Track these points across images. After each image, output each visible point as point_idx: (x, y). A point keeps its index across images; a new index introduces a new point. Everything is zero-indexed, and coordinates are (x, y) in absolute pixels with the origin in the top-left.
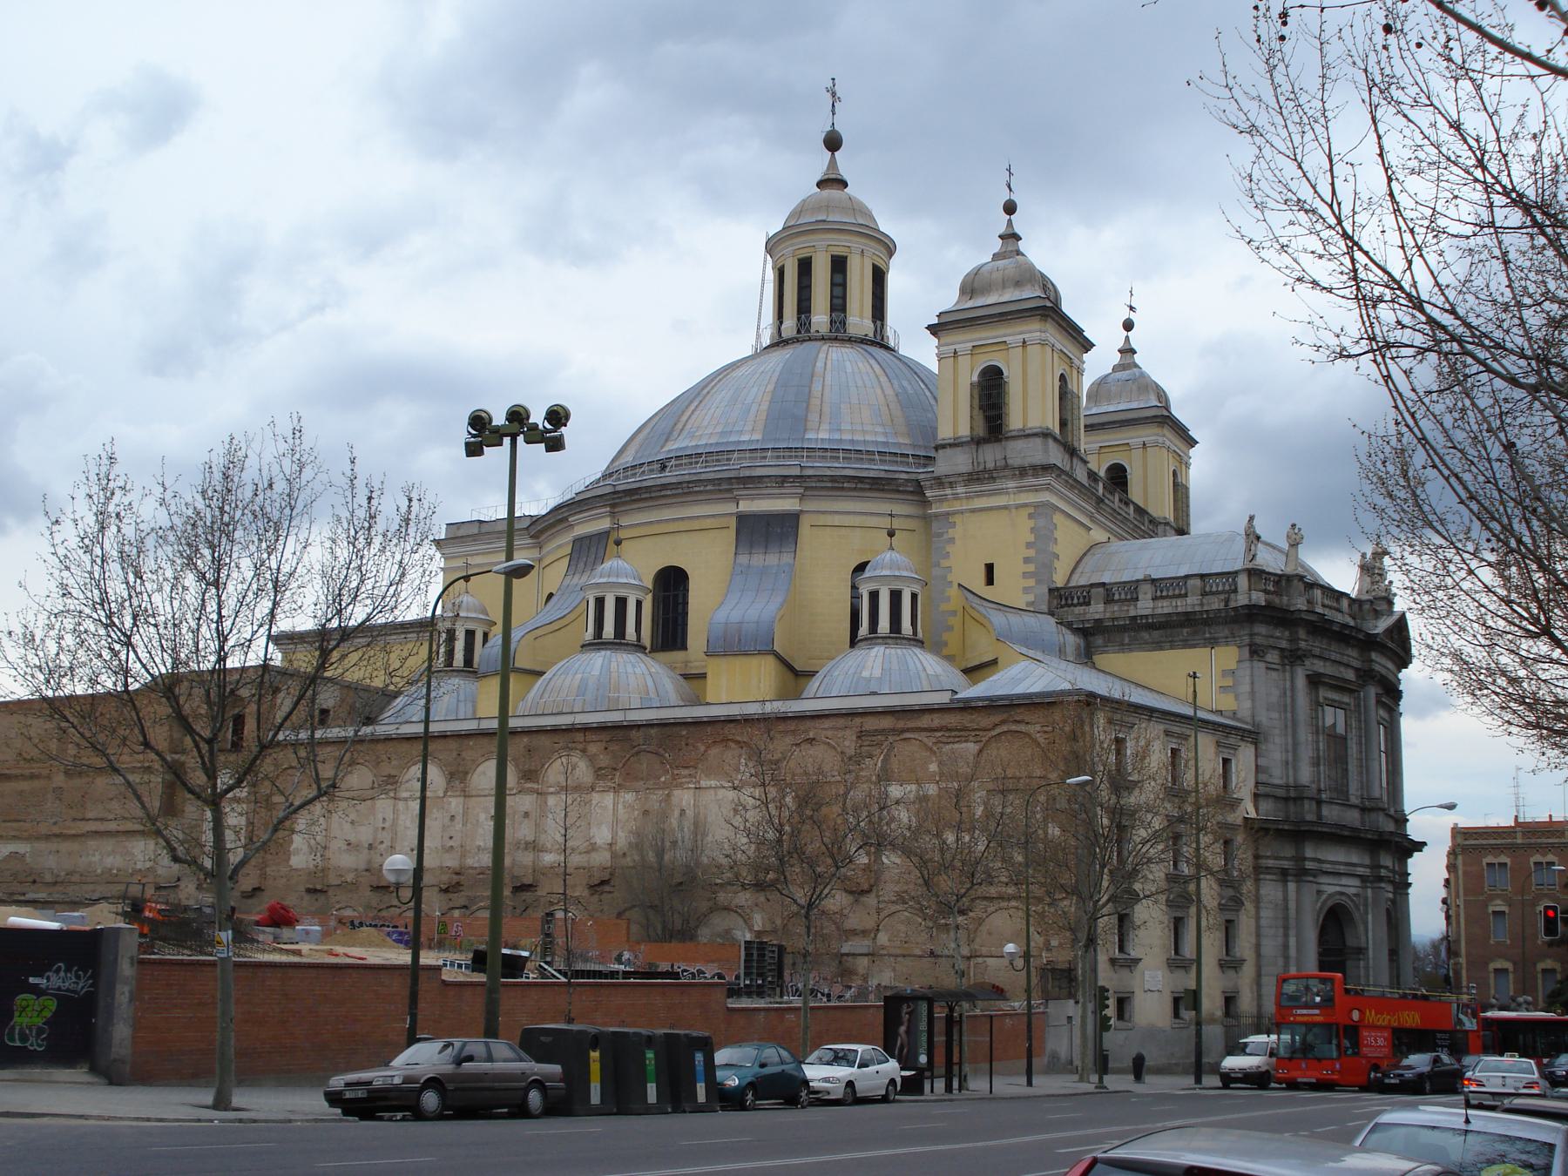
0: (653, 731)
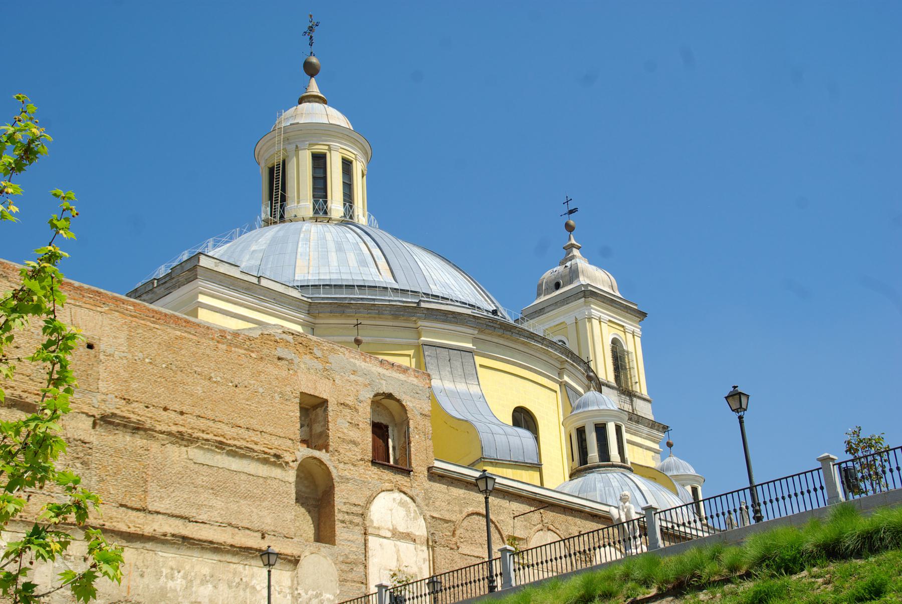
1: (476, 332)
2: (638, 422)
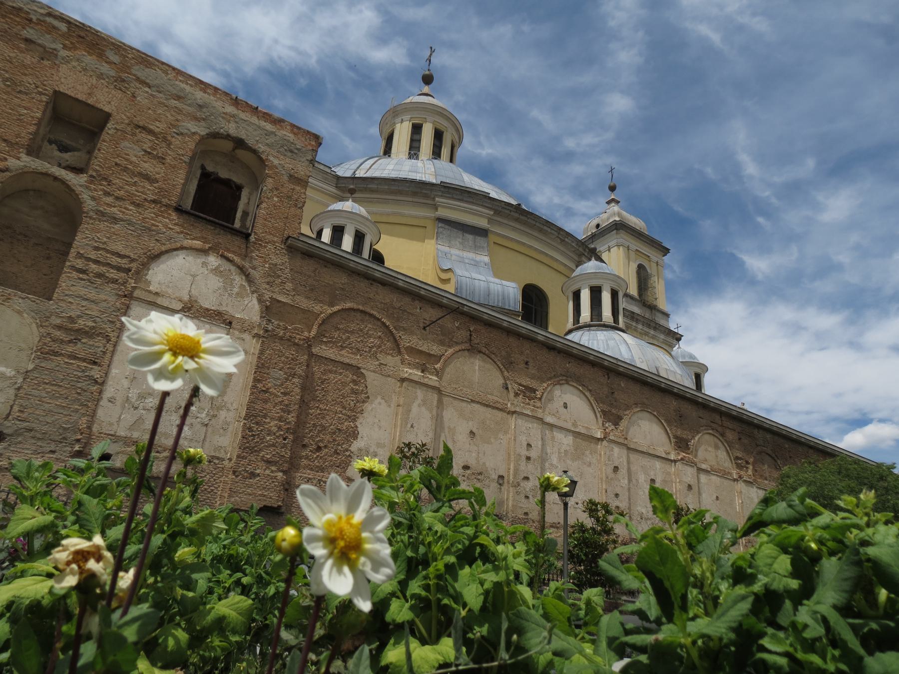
0: (769, 436)
2: (655, 329)
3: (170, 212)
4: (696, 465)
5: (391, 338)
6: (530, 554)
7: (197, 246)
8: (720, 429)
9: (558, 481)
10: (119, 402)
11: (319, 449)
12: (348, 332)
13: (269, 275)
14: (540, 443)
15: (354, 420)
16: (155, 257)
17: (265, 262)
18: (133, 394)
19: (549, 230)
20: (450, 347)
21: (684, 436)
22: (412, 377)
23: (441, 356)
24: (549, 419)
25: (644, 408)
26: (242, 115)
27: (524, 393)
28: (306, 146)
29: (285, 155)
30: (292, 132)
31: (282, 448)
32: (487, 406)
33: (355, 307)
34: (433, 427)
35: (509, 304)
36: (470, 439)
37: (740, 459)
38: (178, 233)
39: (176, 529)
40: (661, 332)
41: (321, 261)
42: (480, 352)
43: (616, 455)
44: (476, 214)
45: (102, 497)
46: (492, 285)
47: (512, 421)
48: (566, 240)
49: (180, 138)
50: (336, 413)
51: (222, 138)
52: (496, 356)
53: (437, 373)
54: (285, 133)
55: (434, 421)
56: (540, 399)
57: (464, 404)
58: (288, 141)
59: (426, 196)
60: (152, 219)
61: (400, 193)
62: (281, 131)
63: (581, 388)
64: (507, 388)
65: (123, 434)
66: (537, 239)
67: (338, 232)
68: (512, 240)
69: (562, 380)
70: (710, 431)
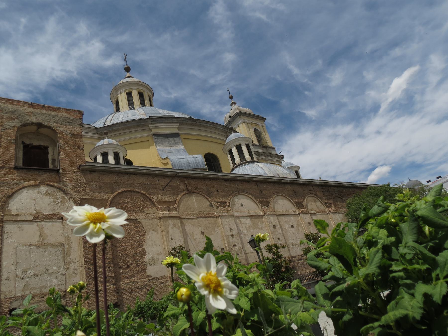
0: (336, 189)
1: (179, 125)
2: (271, 156)
3: (11, 171)
4: (309, 212)
5: (148, 200)
6: (262, 275)
7: (32, 184)
8: (314, 193)
9: (263, 236)
10: (12, 278)
11: (128, 266)
12: (125, 203)
13: (76, 187)
14: (236, 227)
15: (142, 245)
16: (11, 196)
17: (71, 181)
18: (19, 272)
19: (208, 125)
20: (178, 195)
21: (300, 201)
22: (164, 216)
23: (175, 201)
24: (236, 214)
25: (278, 194)
26: (37, 111)
27: (221, 205)
28: (76, 117)
29: (66, 125)
30: (66, 112)
31: (109, 272)
32: (205, 217)
33: (125, 190)
34: (183, 236)
35: (200, 165)
36: (202, 236)
37: (327, 203)
38: (19, 180)
39: (86, 326)
40: (274, 157)
41: (101, 172)
42: (194, 192)
43: (272, 220)
44: (171, 128)
45: (39, 324)
46: (189, 159)
47: (220, 221)
48: (218, 127)
49: (6, 131)
50: (132, 245)
51: (29, 125)
52: (202, 192)
53: (176, 209)
54: (62, 114)
55: (182, 233)
56: (229, 206)
57: (194, 220)
58: (66, 118)
59: (144, 126)
60: (3, 177)
61: (130, 128)
62: (60, 114)
63: (246, 194)
64: (212, 206)
65: (19, 295)
66: (204, 131)
67: (105, 156)
68: (192, 135)
69: (236, 193)
70: (310, 195)
